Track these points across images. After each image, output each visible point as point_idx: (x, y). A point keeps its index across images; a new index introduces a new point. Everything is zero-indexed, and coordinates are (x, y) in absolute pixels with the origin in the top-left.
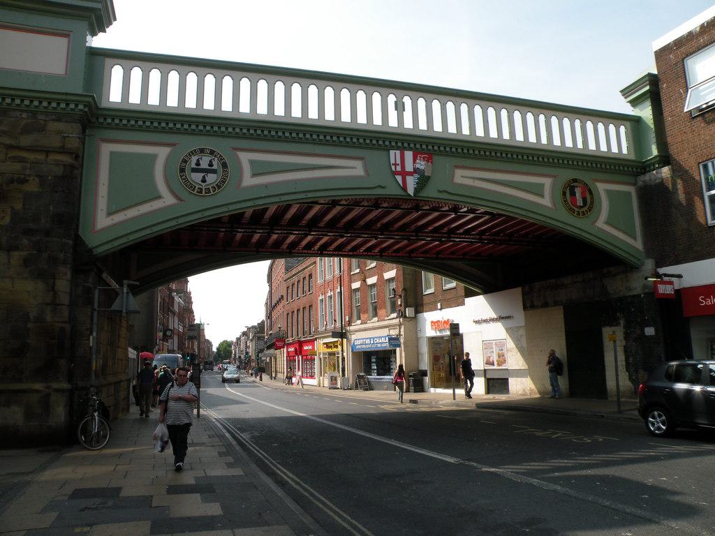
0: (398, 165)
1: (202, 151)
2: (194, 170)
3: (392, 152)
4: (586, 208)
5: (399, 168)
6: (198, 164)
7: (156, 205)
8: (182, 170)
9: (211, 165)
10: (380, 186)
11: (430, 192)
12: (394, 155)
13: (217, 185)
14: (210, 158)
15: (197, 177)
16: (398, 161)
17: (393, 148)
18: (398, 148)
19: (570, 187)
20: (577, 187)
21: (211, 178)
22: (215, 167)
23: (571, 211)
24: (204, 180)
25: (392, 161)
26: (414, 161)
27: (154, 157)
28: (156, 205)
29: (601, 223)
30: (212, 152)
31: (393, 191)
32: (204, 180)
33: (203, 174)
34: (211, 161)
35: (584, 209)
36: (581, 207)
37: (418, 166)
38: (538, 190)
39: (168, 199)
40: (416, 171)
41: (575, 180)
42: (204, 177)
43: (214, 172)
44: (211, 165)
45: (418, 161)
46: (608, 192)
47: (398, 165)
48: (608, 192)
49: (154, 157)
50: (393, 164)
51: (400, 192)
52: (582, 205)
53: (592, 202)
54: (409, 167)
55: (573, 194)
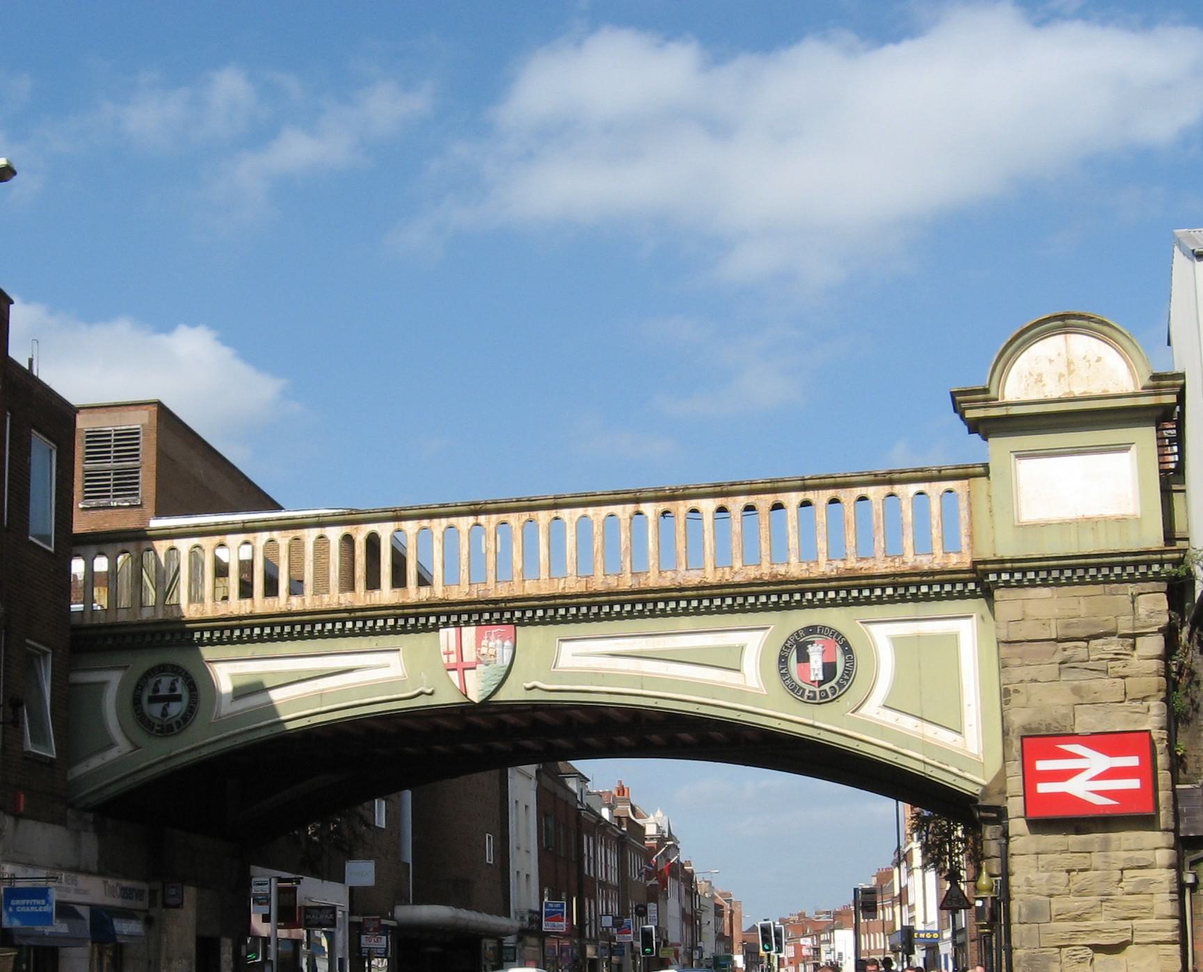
0: (452, 653)
1: (162, 669)
2: (154, 700)
3: (443, 632)
4: (833, 683)
5: (453, 659)
6: (156, 690)
7: (112, 754)
8: (137, 701)
9: (173, 689)
10: (421, 693)
11: (512, 693)
12: (447, 636)
13: (182, 718)
14: (171, 679)
15: (155, 710)
16: (453, 647)
17: (446, 625)
18: (457, 624)
19: (799, 646)
20: (812, 643)
21: (175, 709)
22: (178, 692)
23: (795, 689)
24: (164, 714)
25: (443, 649)
26: (478, 645)
27: (103, 684)
28: (112, 754)
29: (873, 710)
30: (176, 670)
31: (446, 697)
32: (164, 714)
33: (162, 705)
34: (173, 684)
35: (826, 687)
36: (821, 683)
37: (484, 650)
38: (730, 661)
39: (122, 746)
40: (479, 661)
41: (811, 630)
42: (164, 709)
43: (178, 698)
44: (173, 689)
45: (484, 642)
46: (896, 641)
47: (452, 653)
48: (896, 641)
49: (103, 684)
50: (445, 654)
51: (456, 699)
52: (821, 677)
53: (848, 672)
54: (469, 656)
55: (803, 658)
